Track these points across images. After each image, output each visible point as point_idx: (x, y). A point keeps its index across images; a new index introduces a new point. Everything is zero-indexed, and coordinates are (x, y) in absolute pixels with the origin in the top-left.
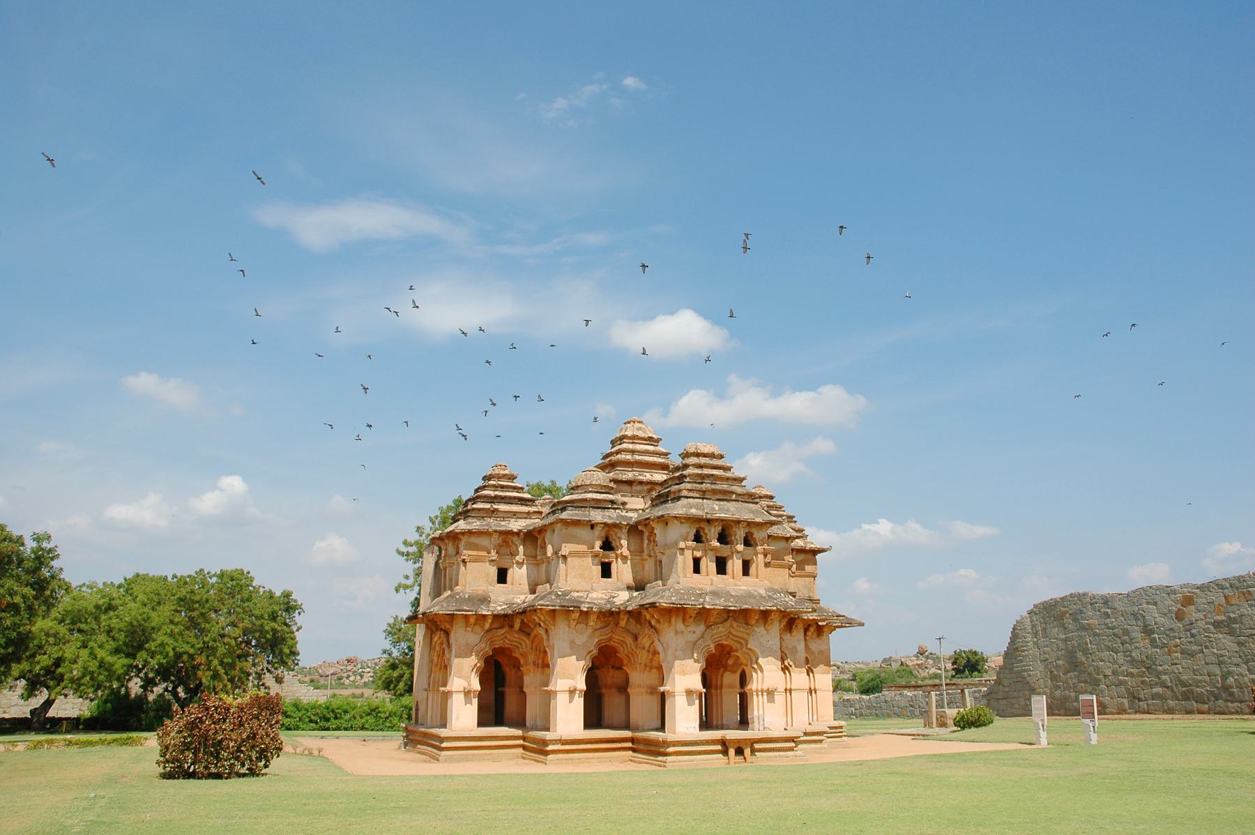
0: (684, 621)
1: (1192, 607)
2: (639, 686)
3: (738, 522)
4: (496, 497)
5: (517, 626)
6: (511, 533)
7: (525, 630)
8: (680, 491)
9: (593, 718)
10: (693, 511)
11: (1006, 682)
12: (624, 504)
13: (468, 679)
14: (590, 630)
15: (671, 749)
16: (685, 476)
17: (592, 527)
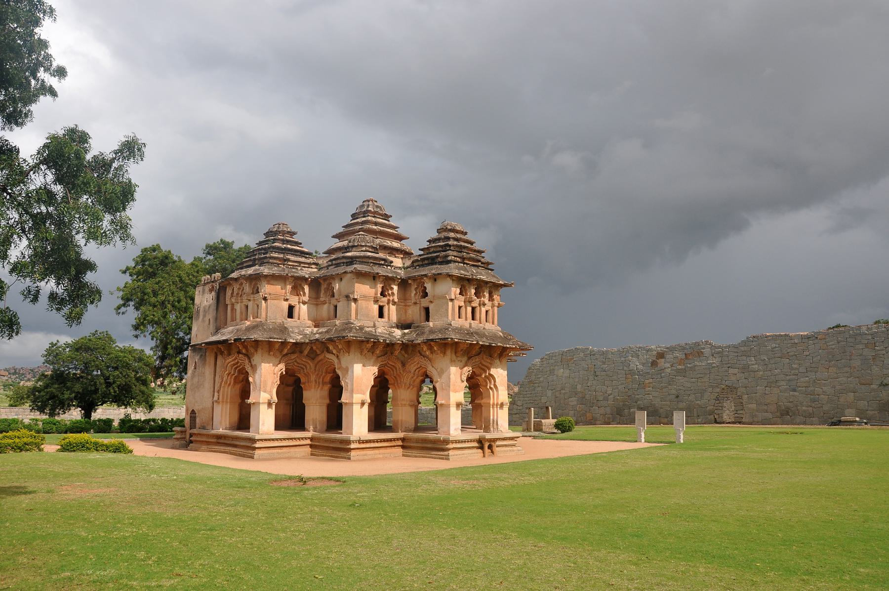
0: (456, 353)
1: (663, 360)
2: (403, 400)
3: (487, 283)
4: (286, 249)
5: (306, 352)
6: (304, 279)
7: (313, 355)
8: (447, 256)
9: (378, 422)
10: (462, 272)
11: (519, 403)
12: (392, 262)
13: (270, 393)
14: (374, 358)
15: (451, 446)
16: (450, 246)
17: (374, 278)
